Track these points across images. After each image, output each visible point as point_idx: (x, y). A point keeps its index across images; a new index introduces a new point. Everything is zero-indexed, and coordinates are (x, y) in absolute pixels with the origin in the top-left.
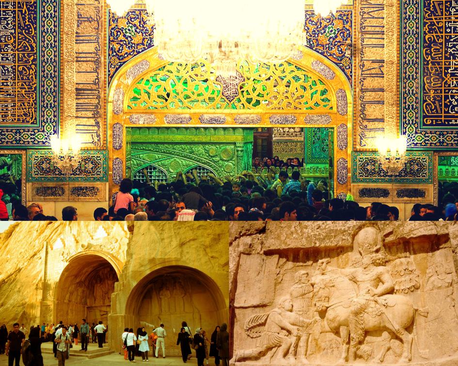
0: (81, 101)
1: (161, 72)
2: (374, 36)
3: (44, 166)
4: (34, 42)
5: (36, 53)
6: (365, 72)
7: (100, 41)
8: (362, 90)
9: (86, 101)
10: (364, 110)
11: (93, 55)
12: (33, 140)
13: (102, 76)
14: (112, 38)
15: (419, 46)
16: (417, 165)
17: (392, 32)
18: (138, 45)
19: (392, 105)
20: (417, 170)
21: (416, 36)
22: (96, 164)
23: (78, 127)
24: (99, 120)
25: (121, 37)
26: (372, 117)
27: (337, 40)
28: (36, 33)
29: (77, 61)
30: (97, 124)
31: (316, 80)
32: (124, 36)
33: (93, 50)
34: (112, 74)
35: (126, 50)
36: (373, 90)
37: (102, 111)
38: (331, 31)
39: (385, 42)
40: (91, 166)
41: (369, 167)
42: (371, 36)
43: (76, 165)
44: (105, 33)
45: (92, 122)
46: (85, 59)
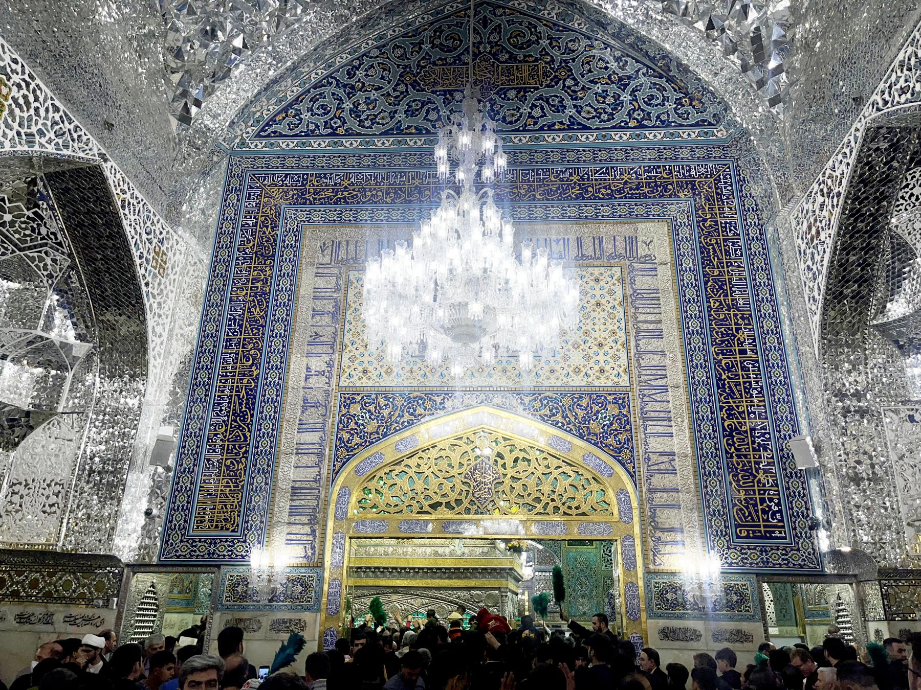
0: (296, 503)
1: (396, 467)
2: (659, 423)
3: (239, 589)
4: (249, 431)
5: (249, 444)
6: (652, 468)
7: (326, 429)
8: (650, 490)
9: (302, 502)
10: (655, 516)
11: (317, 446)
12: (230, 553)
13: (324, 471)
14: (341, 426)
15: (717, 434)
16: (736, 594)
17: (682, 417)
18: (371, 434)
19: (691, 510)
20: (737, 602)
21: (713, 422)
22: (306, 587)
23: (289, 537)
24: (316, 527)
25: (352, 425)
26: (667, 526)
27: (614, 427)
28: (252, 421)
29: (297, 454)
30: (313, 531)
31: (590, 478)
32: (356, 423)
33: (317, 440)
34: (337, 468)
35: (357, 440)
36: (665, 490)
37: (320, 516)
38: (605, 417)
39: (674, 430)
40: (300, 589)
41: (669, 596)
42: (654, 423)
43: (281, 589)
44: (333, 420)
45: (307, 529)
46: (306, 451)
